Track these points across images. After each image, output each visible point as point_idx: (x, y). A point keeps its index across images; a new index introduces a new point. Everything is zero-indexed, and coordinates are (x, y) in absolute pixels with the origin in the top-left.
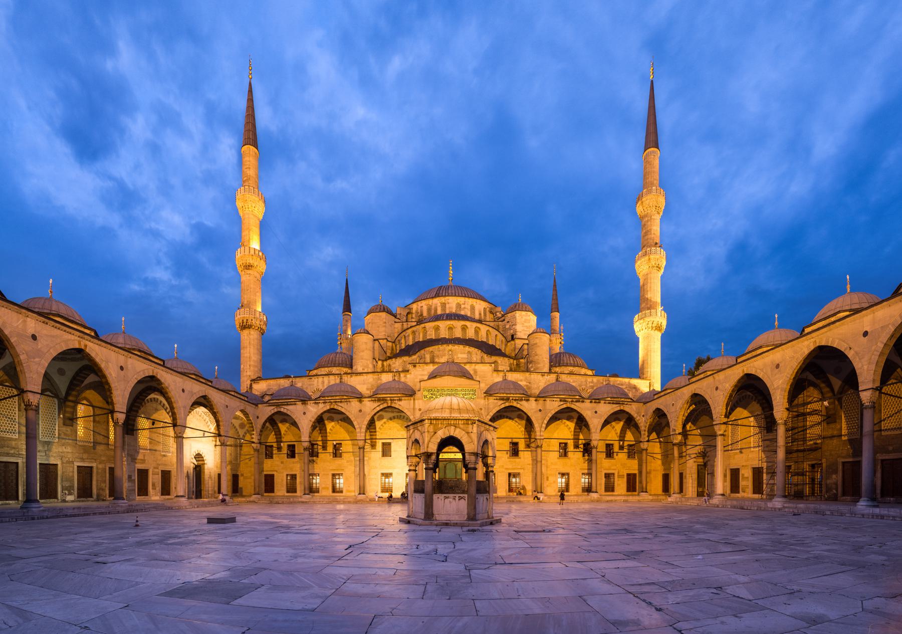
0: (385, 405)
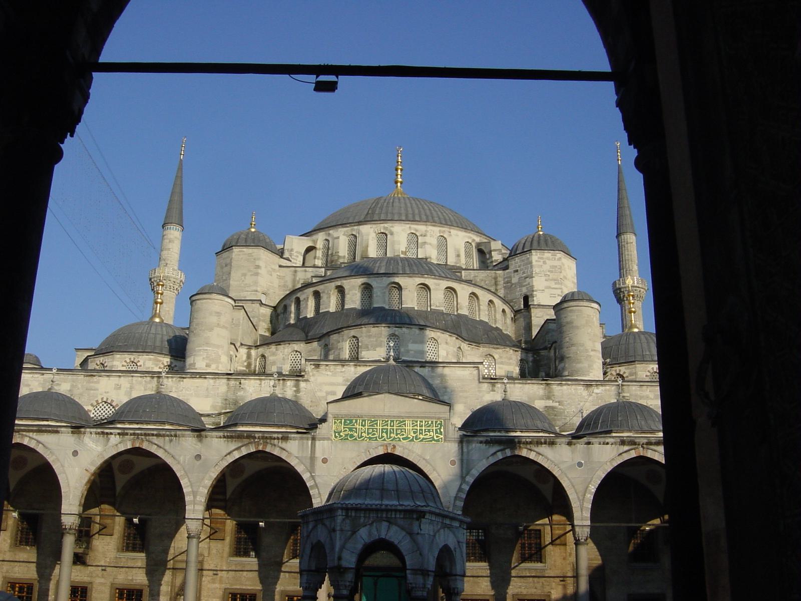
0: (252, 449)
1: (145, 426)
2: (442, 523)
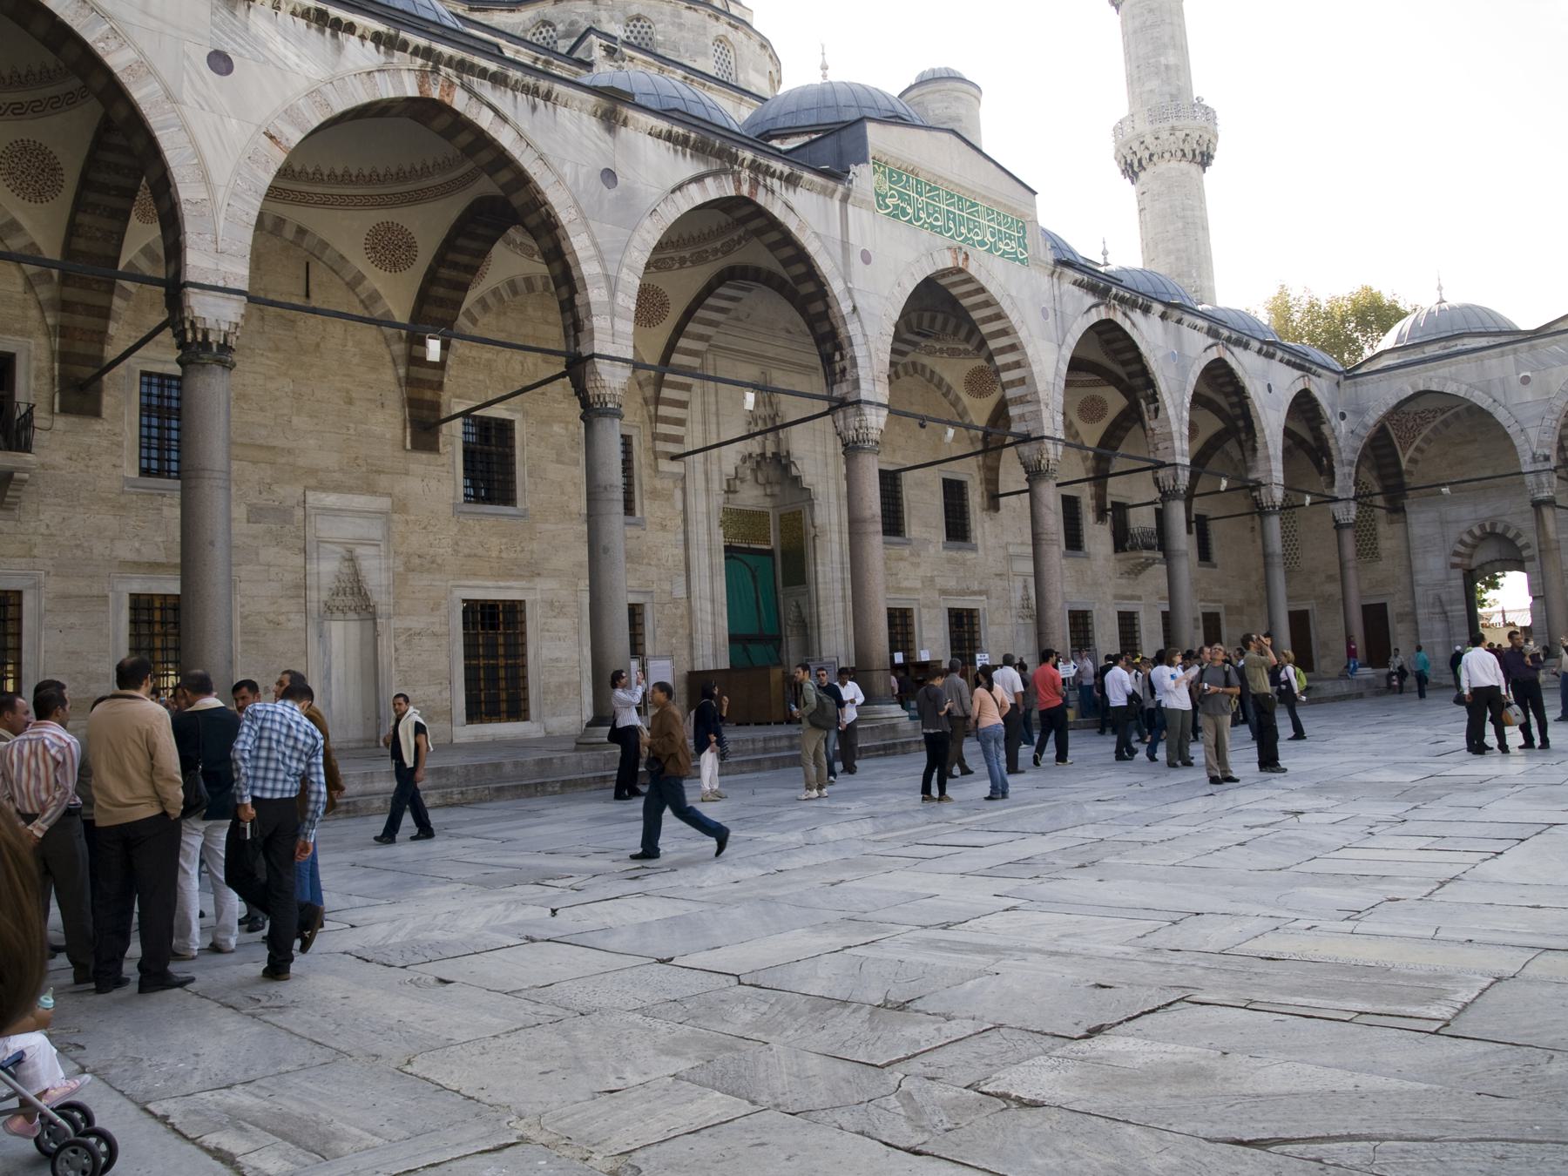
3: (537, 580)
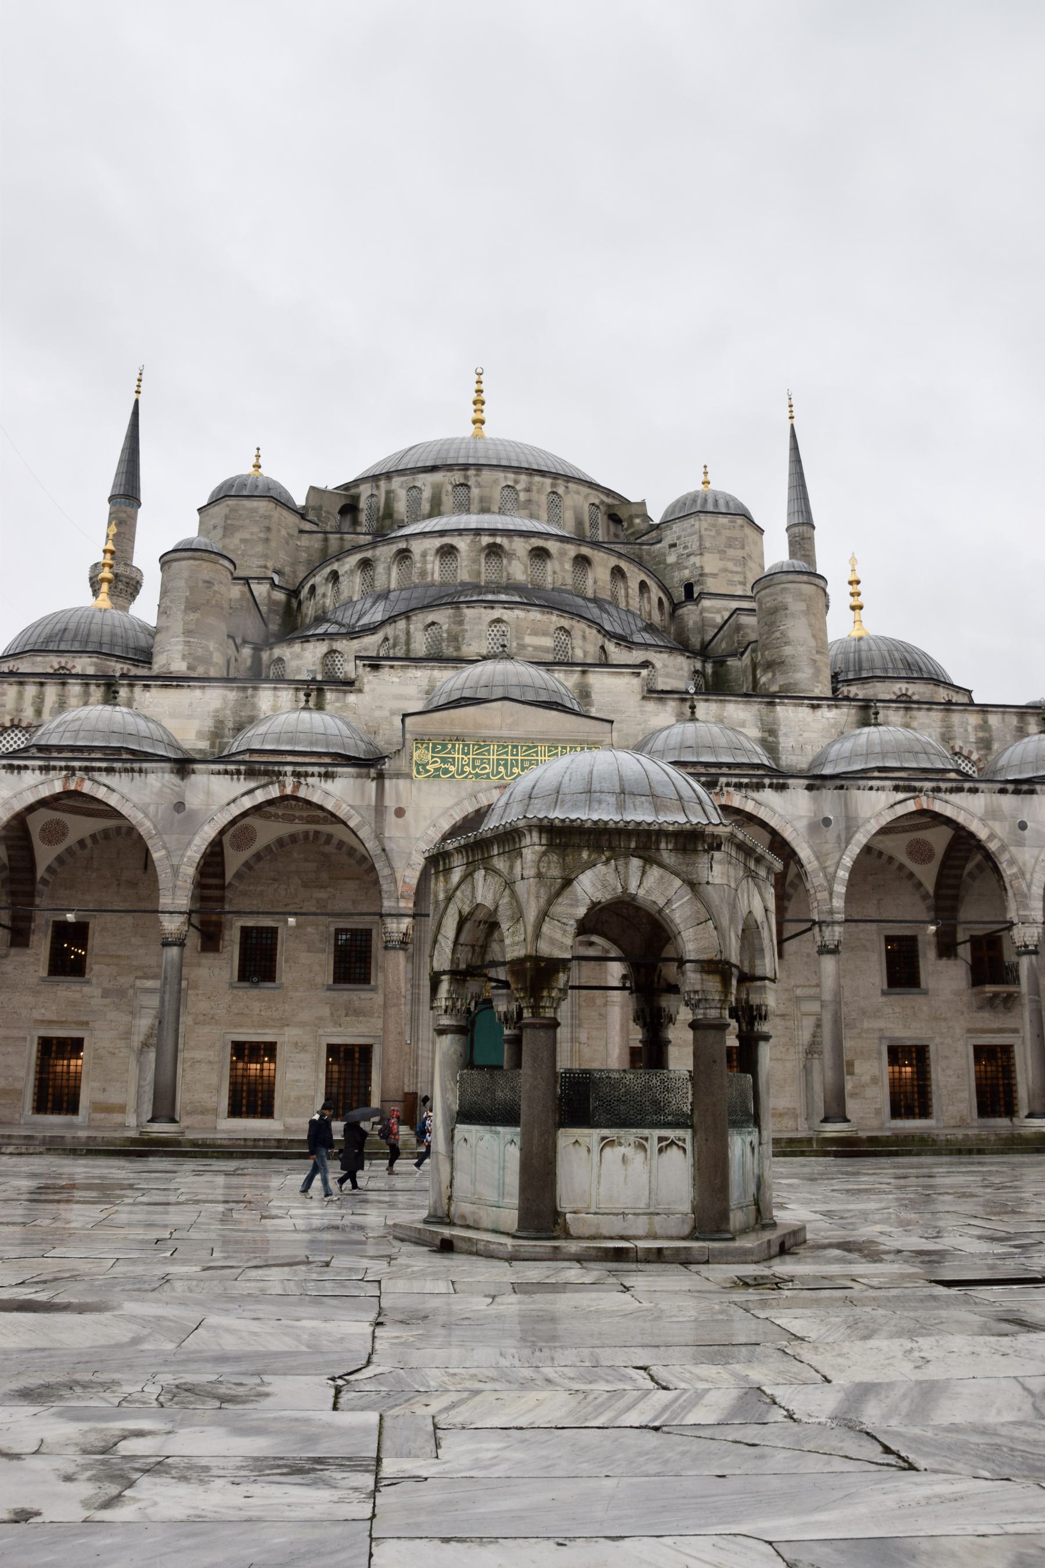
0: (274, 792)
1: (86, 755)
2: (745, 865)
3: (286, 1028)
